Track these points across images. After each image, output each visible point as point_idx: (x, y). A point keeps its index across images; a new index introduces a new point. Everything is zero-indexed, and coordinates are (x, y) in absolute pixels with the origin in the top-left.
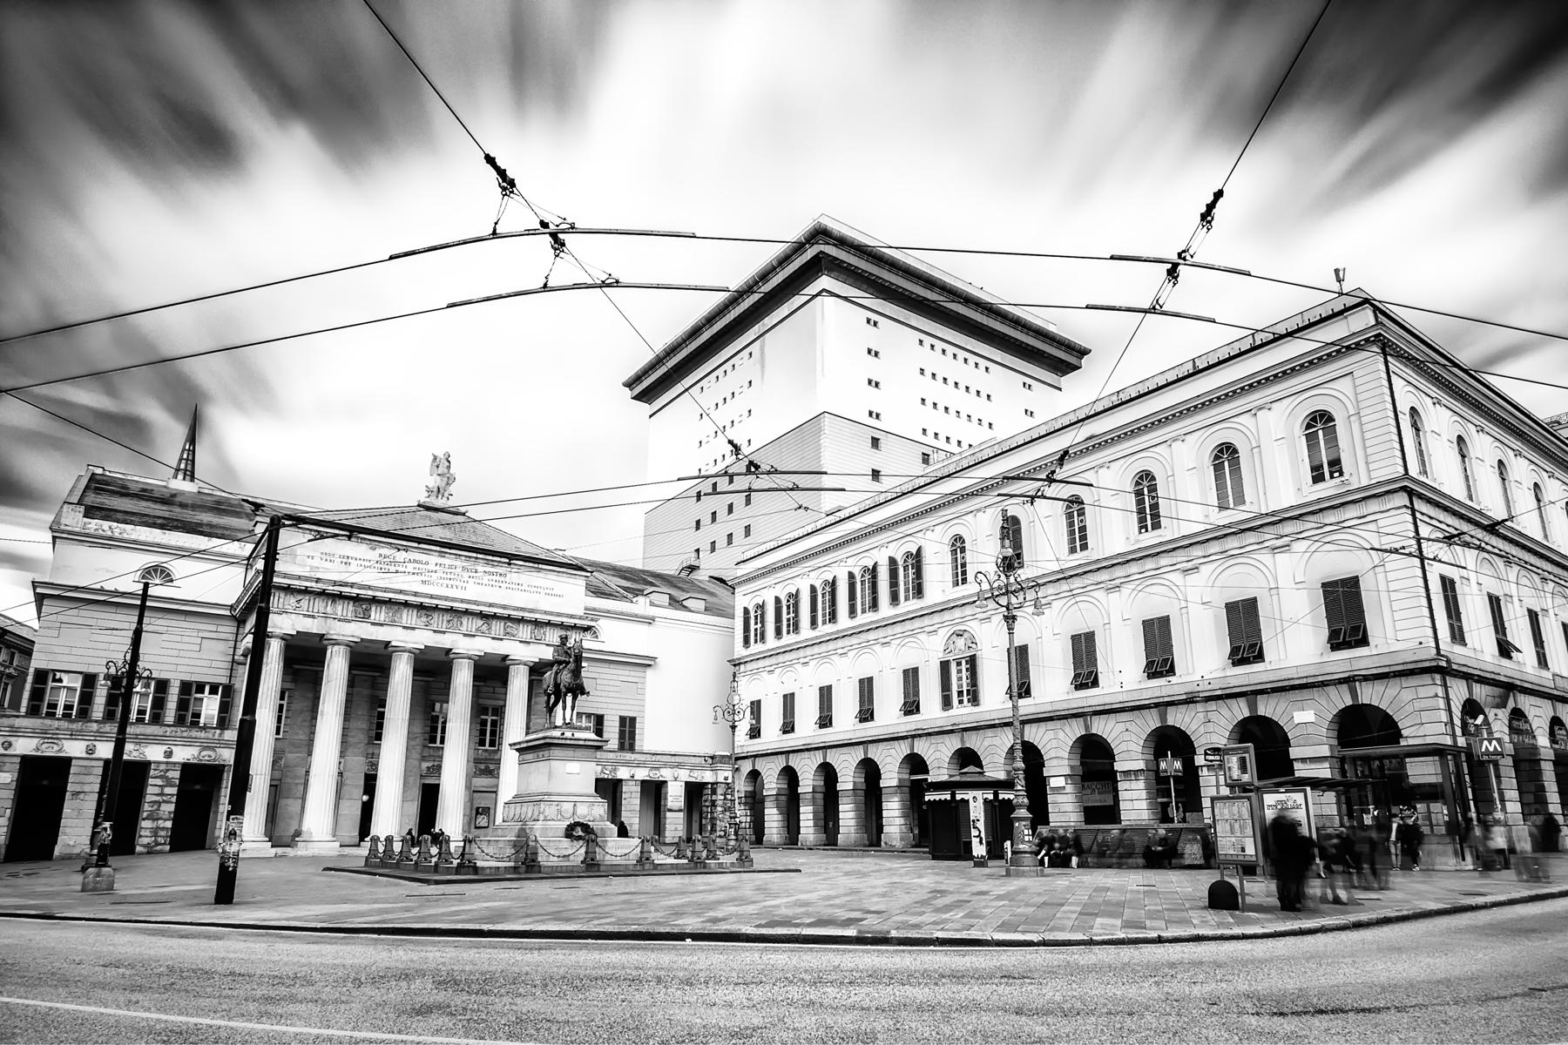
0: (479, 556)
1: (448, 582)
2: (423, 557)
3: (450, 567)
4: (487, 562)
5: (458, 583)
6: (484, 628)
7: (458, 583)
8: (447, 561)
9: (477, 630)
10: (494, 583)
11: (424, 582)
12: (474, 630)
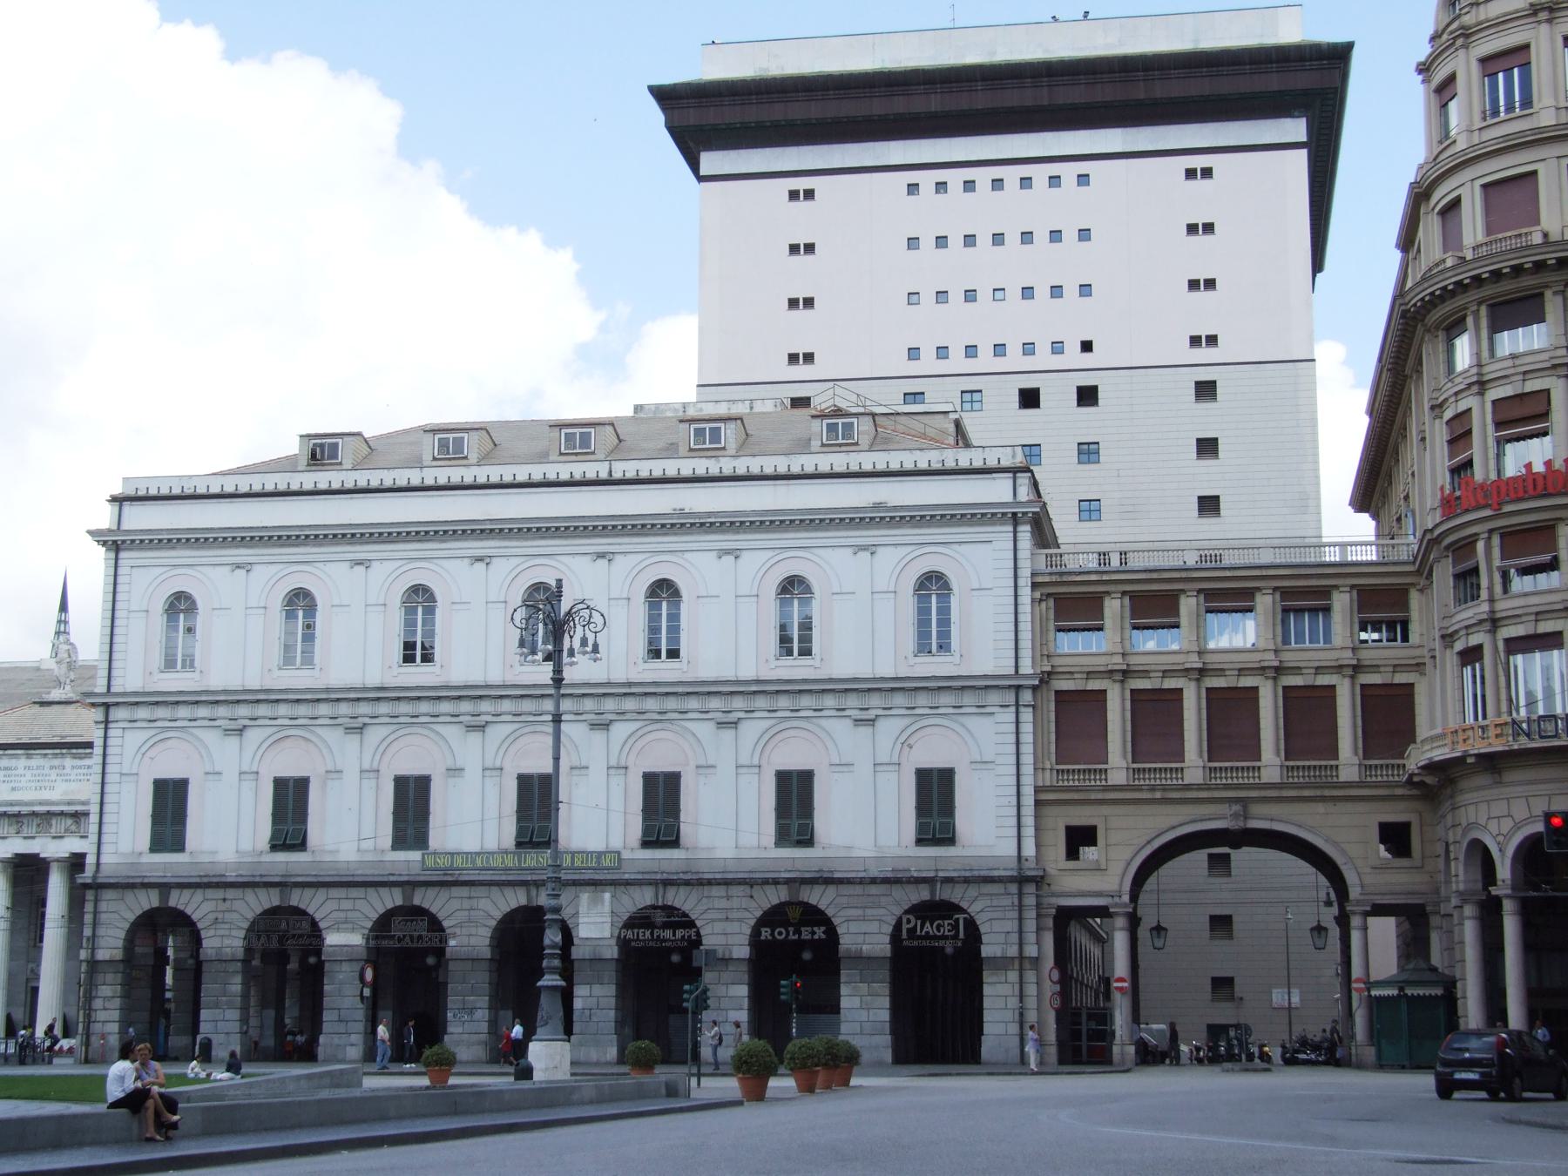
0: (64, 751)
1: (38, 784)
2: (13, 763)
3: (38, 768)
4: (75, 757)
5: (47, 784)
6: (73, 828)
7: (47, 784)
8: (35, 762)
9: (66, 831)
10: (82, 777)
11: (13, 789)
12: (63, 831)
